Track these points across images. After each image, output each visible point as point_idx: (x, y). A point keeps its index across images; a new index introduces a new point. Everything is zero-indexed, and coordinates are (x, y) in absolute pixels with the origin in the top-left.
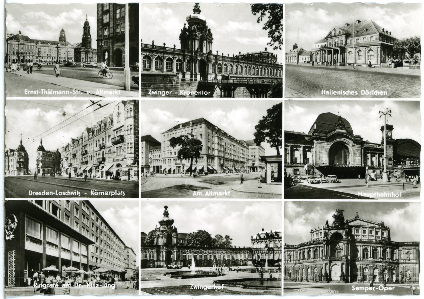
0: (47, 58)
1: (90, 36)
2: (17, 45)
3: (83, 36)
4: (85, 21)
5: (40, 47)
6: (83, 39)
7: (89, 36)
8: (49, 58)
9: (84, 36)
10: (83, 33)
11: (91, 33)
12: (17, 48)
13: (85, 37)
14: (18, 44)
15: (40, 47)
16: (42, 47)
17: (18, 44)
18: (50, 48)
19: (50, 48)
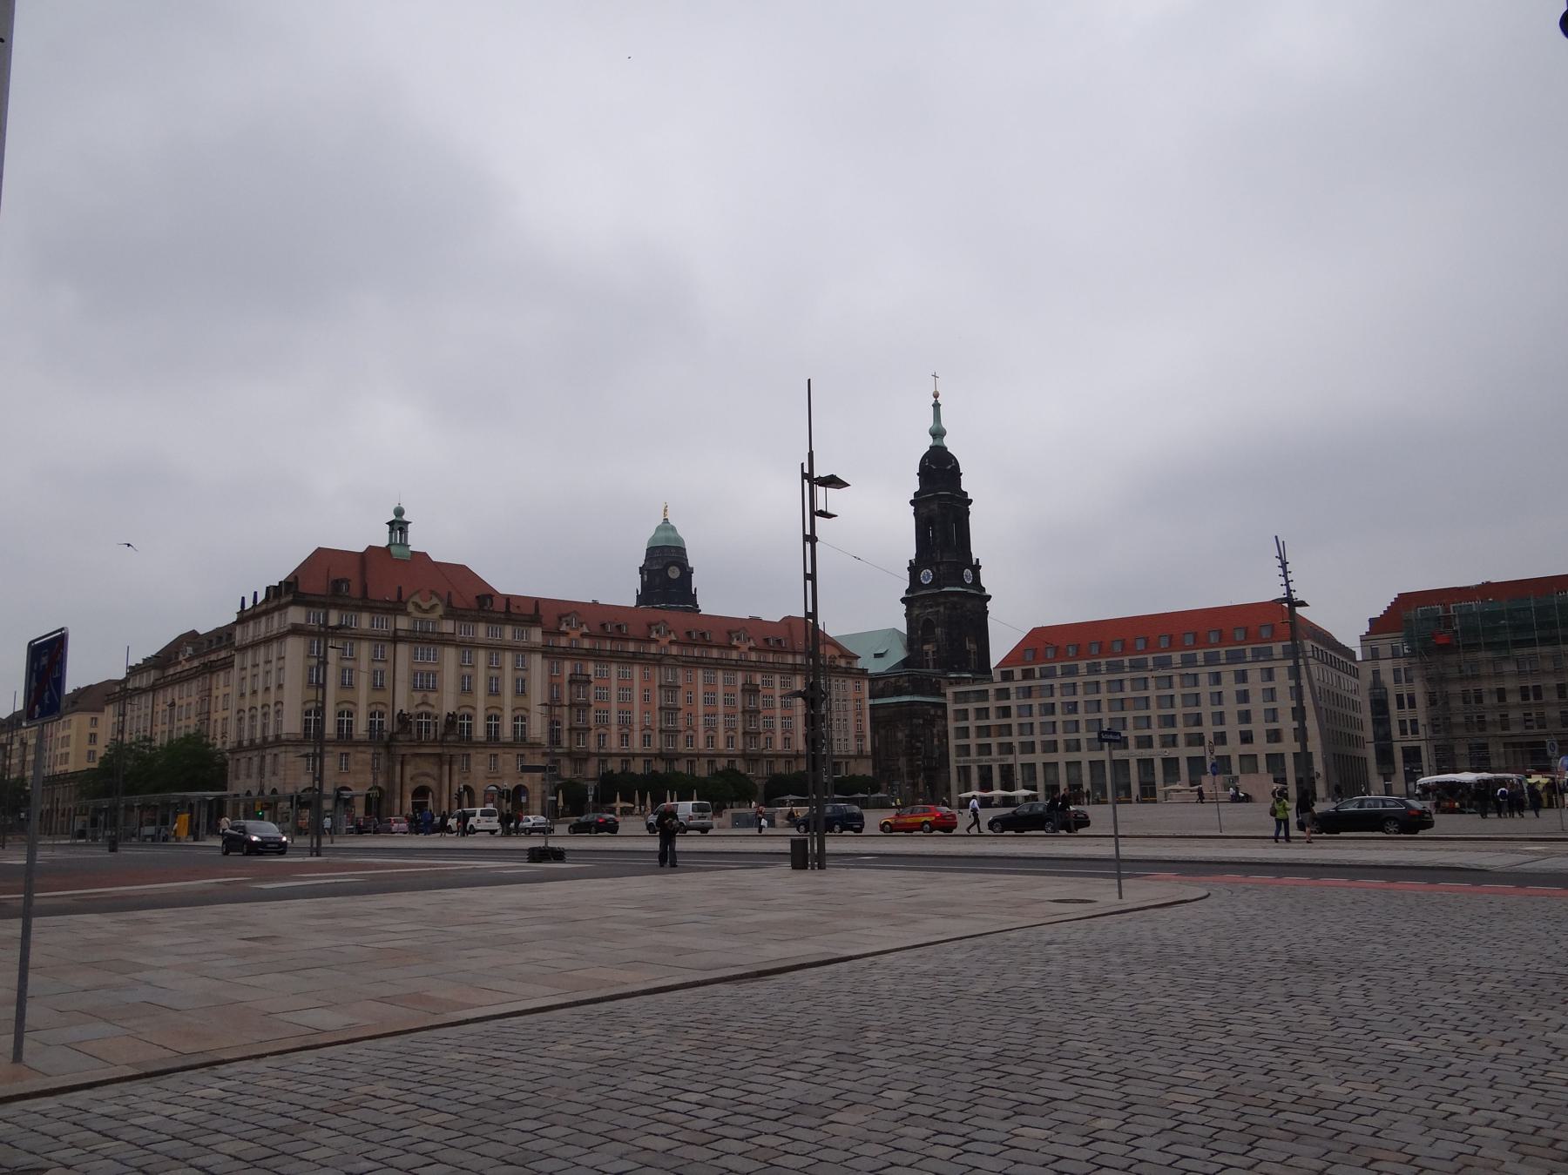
1: (976, 568)
3: (914, 569)
4: (927, 442)
9: (926, 576)
10: (910, 551)
11: (977, 551)
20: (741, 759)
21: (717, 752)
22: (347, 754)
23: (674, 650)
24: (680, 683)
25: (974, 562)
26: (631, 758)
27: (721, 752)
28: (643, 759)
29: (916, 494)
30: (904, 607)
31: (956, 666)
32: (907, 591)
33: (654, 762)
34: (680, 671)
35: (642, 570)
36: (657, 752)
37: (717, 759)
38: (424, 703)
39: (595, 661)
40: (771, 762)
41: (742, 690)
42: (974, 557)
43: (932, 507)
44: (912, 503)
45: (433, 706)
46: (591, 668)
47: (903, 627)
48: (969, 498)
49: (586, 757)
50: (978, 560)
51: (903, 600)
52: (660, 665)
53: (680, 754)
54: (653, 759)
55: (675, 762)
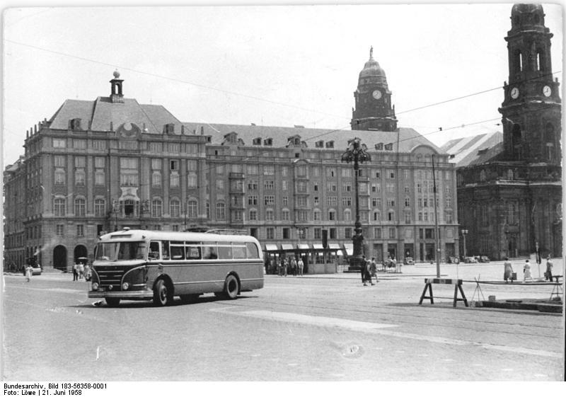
0: (286, 235)
1: (554, 86)
2: (100, 163)
3: (507, 89)
5: (236, 169)
6: (508, 109)
7: (547, 91)
8: (294, 233)
9: (515, 94)
10: (504, 75)
12: (100, 180)
13: (523, 94)
14: (108, 156)
15: (236, 169)
16: (252, 170)
17: (108, 156)
18: (301, 171)
19: (301, 171)
22: (82, 226)
25: (554, 81)
29: (509, 33)
30: (501, 115)
31: (536, 158)
32: (503, 104)
35: (356, 94)
38: (128, 194)
40: (379, 229)
42: (554, 76)
43: (518, 42)
44: (506, 39)
45: (134, 196)
47: (501, 129)
48: (551, 32)
50: (557, 79)
51: (500, 110)
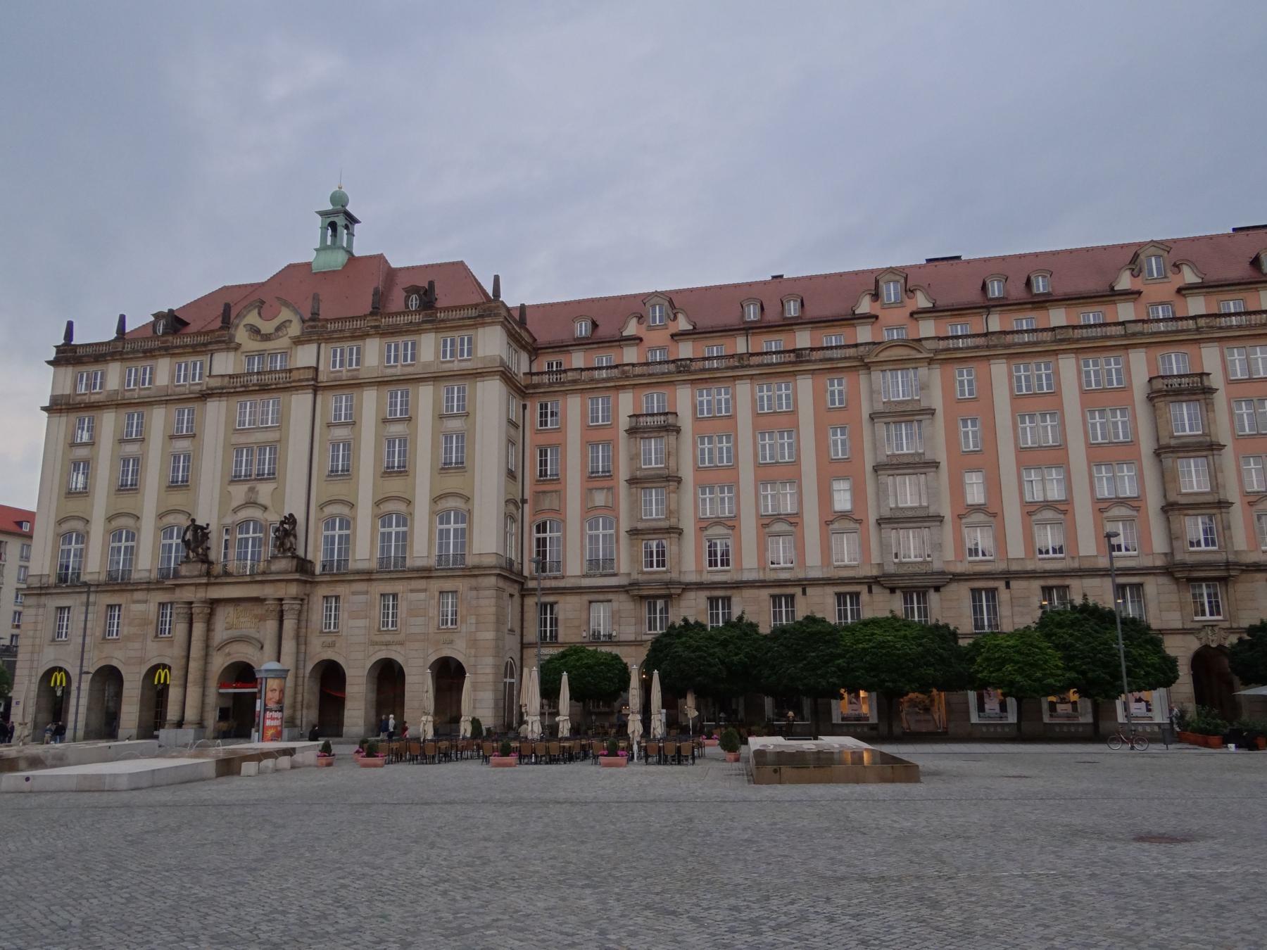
20: (1163, 580)
21: (1076, 565)
23: (927, 328)
24: (937, 402)
26: (798, 591)
27: (1086, 565)
28: (830, 591)
33: (864, 597)
34: (935, 376)
36: (875, 572)
37: (1068, 582)
39: (692, 382)
41: (1150, 398)
46: (684, 399)
49: (672, 592)
52: (867, 367)
53: (943, 573)
54: (864, 589)
55: (932, 592)
